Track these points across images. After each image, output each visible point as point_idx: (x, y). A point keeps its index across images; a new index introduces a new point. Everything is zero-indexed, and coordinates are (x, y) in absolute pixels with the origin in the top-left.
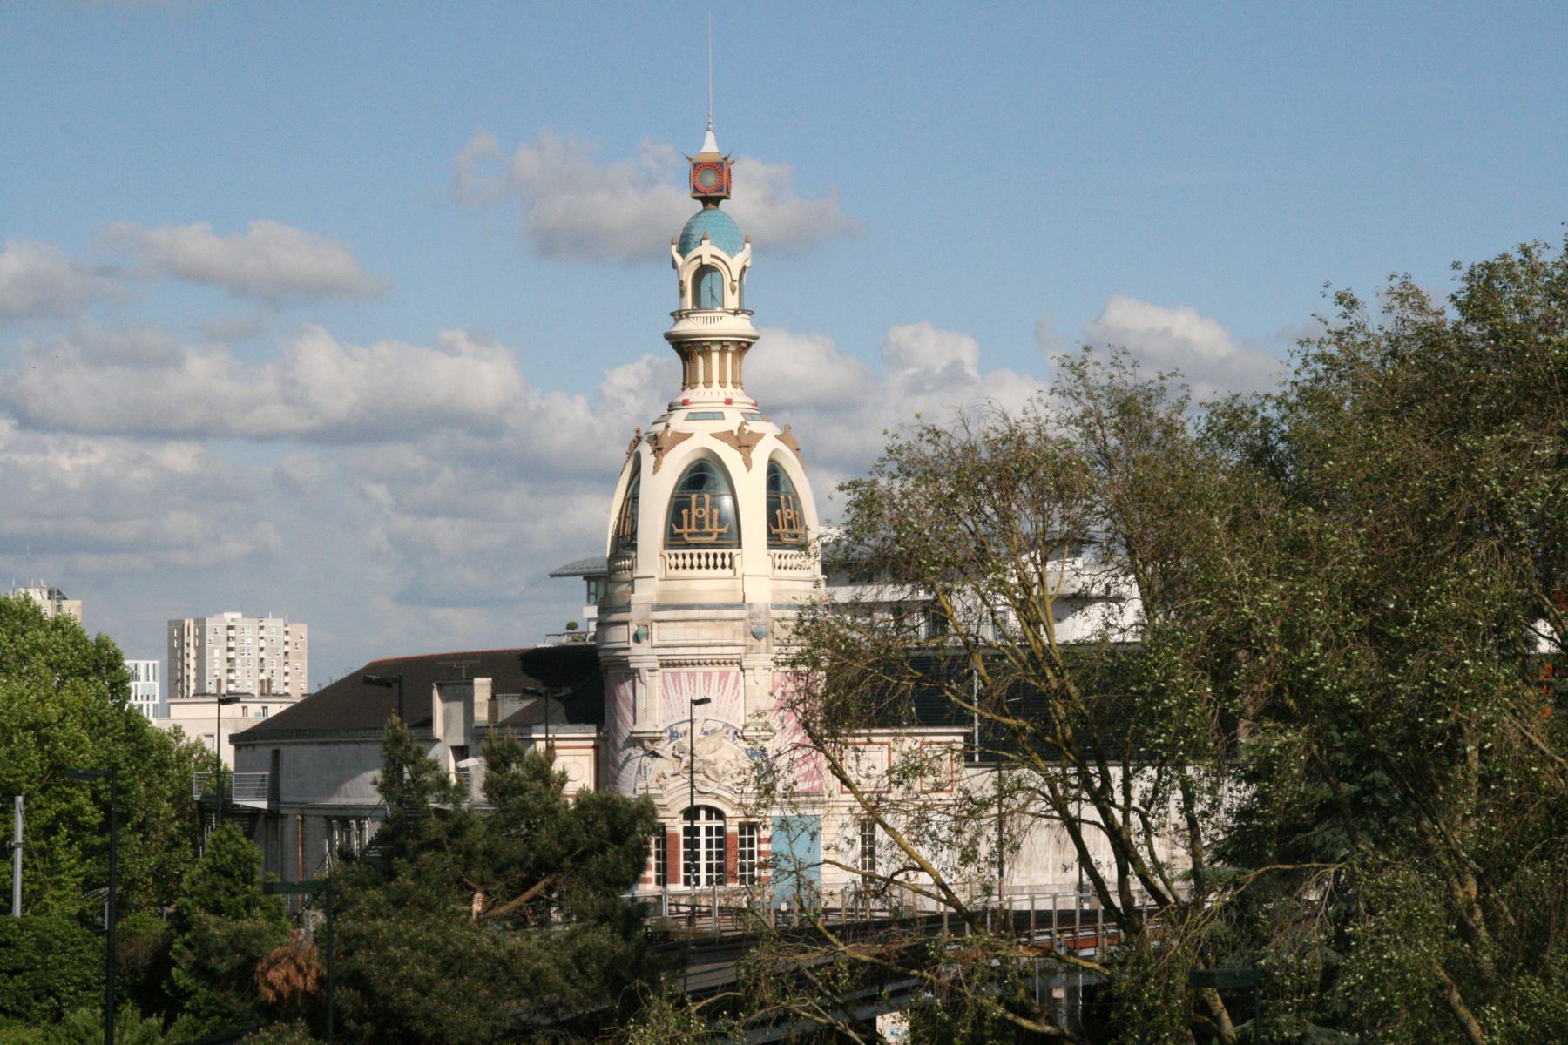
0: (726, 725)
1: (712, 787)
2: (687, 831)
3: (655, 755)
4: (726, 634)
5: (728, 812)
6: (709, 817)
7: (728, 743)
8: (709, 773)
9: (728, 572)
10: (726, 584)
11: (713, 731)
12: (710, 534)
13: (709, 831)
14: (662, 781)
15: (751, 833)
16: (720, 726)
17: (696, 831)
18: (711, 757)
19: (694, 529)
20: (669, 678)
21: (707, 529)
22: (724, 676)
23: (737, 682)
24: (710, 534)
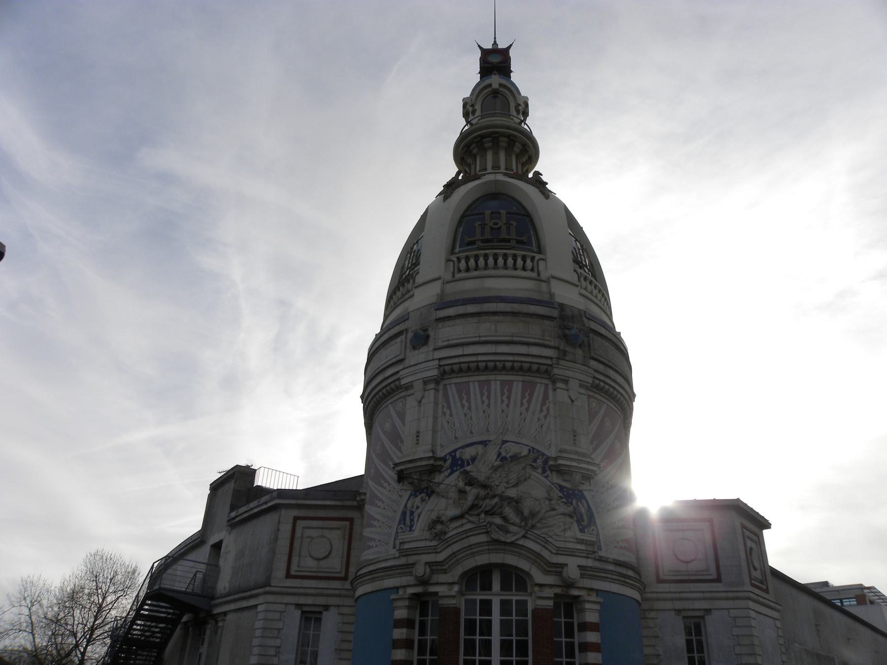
0: (532, 450)
1: (514, 534)
2: (470, 603)
3: (430, 493)
4: (534, 330)
5: (539, 577)
6: (506, 587)
7: (537, 475)
8: (508, 511)
9: (534, 275)
10: (529, 284)
11: (515, 458)
12: (508, 241)
13: (505, 606)
14: (439, 527)
15: (569, 614)
16: (525, 452)
17: (486, 606)
18: (512, 493)
19: (488, 236)
20: (452, 391)
21: (504, 235)
22: (529, 388)
23: (546, 397)
24: (508, 241)
